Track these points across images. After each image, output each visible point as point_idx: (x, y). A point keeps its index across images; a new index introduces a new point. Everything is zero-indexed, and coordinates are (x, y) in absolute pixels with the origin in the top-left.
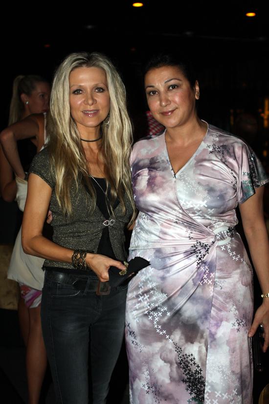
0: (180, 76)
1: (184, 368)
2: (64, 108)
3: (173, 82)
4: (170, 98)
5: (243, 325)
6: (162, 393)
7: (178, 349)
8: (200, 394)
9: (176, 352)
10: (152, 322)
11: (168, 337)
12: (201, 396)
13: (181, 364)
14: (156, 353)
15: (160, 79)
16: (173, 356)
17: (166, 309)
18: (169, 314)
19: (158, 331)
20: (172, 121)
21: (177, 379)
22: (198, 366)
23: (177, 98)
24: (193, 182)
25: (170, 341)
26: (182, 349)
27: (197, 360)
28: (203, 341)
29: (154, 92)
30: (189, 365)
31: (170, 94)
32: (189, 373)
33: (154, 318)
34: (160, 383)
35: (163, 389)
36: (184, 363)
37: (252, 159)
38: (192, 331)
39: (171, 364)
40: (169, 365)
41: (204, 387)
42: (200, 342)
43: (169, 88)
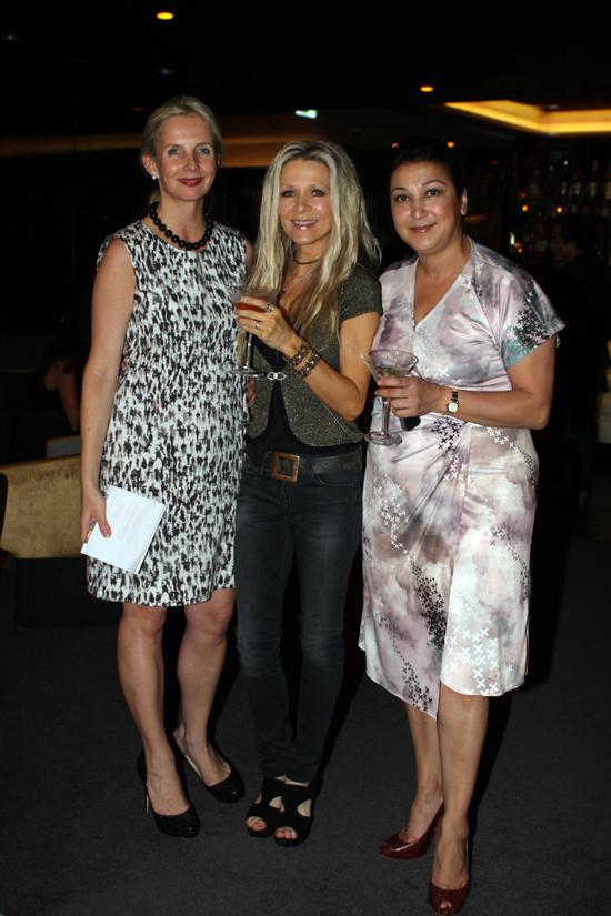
0: (444, 179)
2: (270, 219)
3: (433, 186)
4: (427, 208)
5: (503, 537)
6: (398, 628)
7: (417, 569)
14: (392, 573)
15: (415, 179)
16: (411, 579)
17: (404, 513)
20: (424, 243)
22: (440, 596)
23: (436, 207)
24: (434, 340)
27: (439, 588)
28: (448, 560)
29: (404, 197)
31: (427, 202)
34: (395, 614)
35: (398, 623)
37: (529, 300)
38: (434, 546)
39: (408, 590)
43: (427, 193)
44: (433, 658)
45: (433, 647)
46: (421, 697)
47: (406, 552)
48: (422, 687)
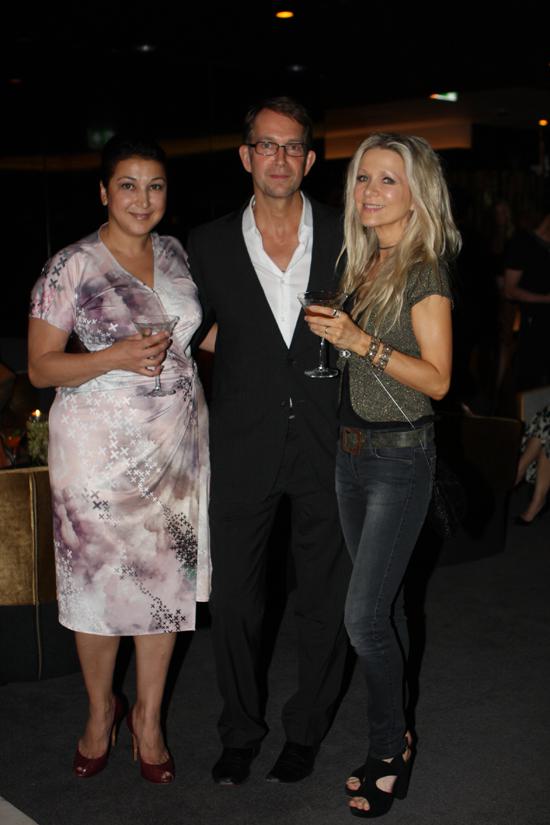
6: (147, 571)
10: (135, 485)
11: (155, 499)
14: (139, 524)
16: (162, 522)
18: (158, 470)
19: (144, 495)
21: (165, 548)
25: (159, 503)
28: (194, 493)
33: (138, 479)
34: (143, 559)
39: (158, 531)
42: (191, 496)
44: (184, 580)
45: (184, 571)
46: (171, 621)
47: (155, 499)
48: (173, 612)
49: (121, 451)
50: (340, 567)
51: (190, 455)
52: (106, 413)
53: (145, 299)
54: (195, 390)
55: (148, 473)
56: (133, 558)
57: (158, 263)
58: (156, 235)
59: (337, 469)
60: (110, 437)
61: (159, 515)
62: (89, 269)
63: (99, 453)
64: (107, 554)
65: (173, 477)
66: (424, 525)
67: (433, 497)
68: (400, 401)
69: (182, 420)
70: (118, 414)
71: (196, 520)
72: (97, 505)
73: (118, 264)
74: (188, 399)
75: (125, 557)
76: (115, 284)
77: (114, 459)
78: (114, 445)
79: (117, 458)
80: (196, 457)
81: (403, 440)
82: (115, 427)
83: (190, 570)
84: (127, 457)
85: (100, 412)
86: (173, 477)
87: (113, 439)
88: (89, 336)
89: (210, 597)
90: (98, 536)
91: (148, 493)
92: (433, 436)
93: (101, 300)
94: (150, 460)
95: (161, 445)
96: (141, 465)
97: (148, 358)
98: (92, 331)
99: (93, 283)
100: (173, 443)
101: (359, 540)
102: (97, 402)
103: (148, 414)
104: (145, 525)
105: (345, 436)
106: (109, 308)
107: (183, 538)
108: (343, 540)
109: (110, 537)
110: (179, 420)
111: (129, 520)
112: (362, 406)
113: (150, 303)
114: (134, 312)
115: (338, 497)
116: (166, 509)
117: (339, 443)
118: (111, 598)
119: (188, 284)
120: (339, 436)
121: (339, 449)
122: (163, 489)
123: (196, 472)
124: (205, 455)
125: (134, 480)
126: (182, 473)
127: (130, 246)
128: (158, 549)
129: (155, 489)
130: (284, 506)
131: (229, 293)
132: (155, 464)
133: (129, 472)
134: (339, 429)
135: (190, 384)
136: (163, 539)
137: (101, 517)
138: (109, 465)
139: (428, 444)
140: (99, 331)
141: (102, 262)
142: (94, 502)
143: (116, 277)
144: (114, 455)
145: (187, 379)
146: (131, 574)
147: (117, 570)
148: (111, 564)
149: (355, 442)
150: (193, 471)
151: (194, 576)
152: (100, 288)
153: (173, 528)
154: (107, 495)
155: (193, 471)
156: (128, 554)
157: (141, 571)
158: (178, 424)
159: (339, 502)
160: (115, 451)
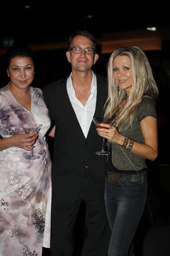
1: (35, 217)
6: (22, 234)
8: (42, 228)
9: (32, 210)
10: (20, 195)
11: (28, 202)
12: (42, 229)
13: (33, 215)
14: (21, 213)
16: (31, 212)
18: (31, 190)
19: (24, 200)
25: (30, 204)
26: (35, 207)
28: (45, 200)
30: (38, 215)
32: (37, 219)
33: (22, 193)
34: (22, 228)
36: (35, 214)
39: (28, 216)
40: (28, 217)
41: (44, 224)
42: (43, 201)
44: (38, 238)
45: (38, 234)
47: (28, 202)
49: (15, 181)
50: (106, 232)
51: (44, 183)
52: (9, 164)
53: (27, 116)
54: (47, 156)
55: (26, 190)
56: (17, 228)
57: (33, 100)
58: (32, 88)
59: (105, 190)
60: (11, 174)
61: (29, 209)
62: (4, 102)
63: (5, 181)
64: (6, 226)
65: (36, 193)
66: (142, 216)
67: (146, 202)
68: (133, 161)
69: (42, 169)
70: (14, 164)
71: (45, 212)
72: (3, 204)
73: (16, 100)
74: (44, 159)
75: (14, 228)
76: (14, 110)
77: (12, 184)
78: (12, 178)
79: (13, 184)
80: (46, 184)
81: (133, 179)
82: (13, 170)
83: (41, 234)
84: (17, 183)
85: (6, 163)
86: (36, 193)
87: (12, 175)
88: (3, 131)
89: (50, 246)
90: (3, 218)
91: (25, 200)
92: (146, 177)
93: (8, 116)
94: (27, 185)
95: (32, 178)
96: (23, 187)
97: (28, 143)
98: (4, 130)
99: (5, 109)
100: (37, 178)
101: (114, 222)
102: (5, 159)
103: (28, 165)
104: (23, 214)
105: (109, 175)
106: (12, 120)
107: (39, 219)
108: (108, 221)
109: (8, 218)
110: (41, 167)
111: (16, 211)
112: (117, 163)
113: (29, 118)
114: (23, 122)
115: (106, 202)
116: (33, 207)
117: (106, 178)
118: (7, 245)
119: (45, 110)
120: (106, 175)
121: (106, 181)
122: (32, 198)
123: (46, 191)
124: (50, 184)
125: (20, 193)
126: (40, 191)
127: (21, 93)
128: (28, 225)
129: (28, 198)
130: (83, 205)
131: (61, 113)
132: (29, 187)
133: (18, 190)
134: (106, 173)
135: (45, 153)
136: (31, 219)
137: (5, 209)
138: (9, 187)
139: (144, 180)
140: (7, 130)
141: (9, 99)
142: (2, 203)
143: (15, 106)
144: (12, 182)
145: (44, 151)
146: (16, 235)
147: (10, 233)
148: (7, 230)
149: (113, 178)
150: (45, 191)
151: (42, 236)
152: (8, 111)
153: (35, 215)
154: (8, 200)
155: (45, 191)
156: (15, 226)
157: (20, 234)
158: (40, 170)
159: (106, 204)
160: (12, 180)
